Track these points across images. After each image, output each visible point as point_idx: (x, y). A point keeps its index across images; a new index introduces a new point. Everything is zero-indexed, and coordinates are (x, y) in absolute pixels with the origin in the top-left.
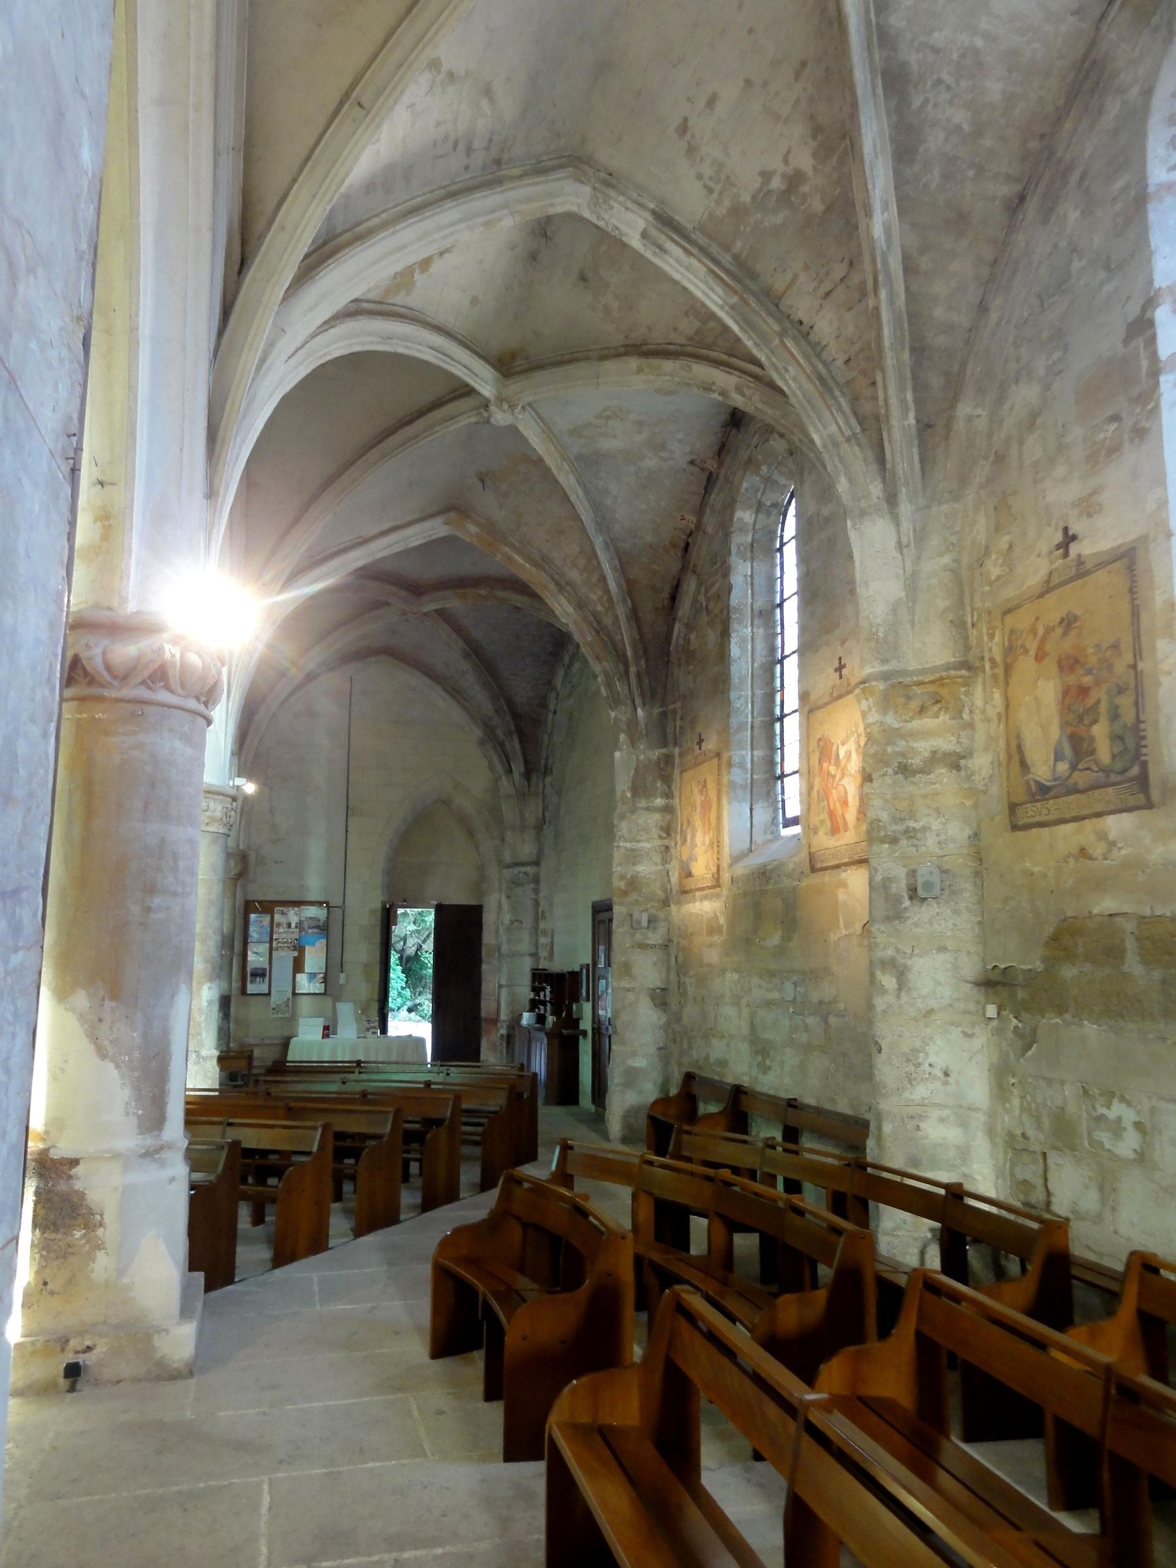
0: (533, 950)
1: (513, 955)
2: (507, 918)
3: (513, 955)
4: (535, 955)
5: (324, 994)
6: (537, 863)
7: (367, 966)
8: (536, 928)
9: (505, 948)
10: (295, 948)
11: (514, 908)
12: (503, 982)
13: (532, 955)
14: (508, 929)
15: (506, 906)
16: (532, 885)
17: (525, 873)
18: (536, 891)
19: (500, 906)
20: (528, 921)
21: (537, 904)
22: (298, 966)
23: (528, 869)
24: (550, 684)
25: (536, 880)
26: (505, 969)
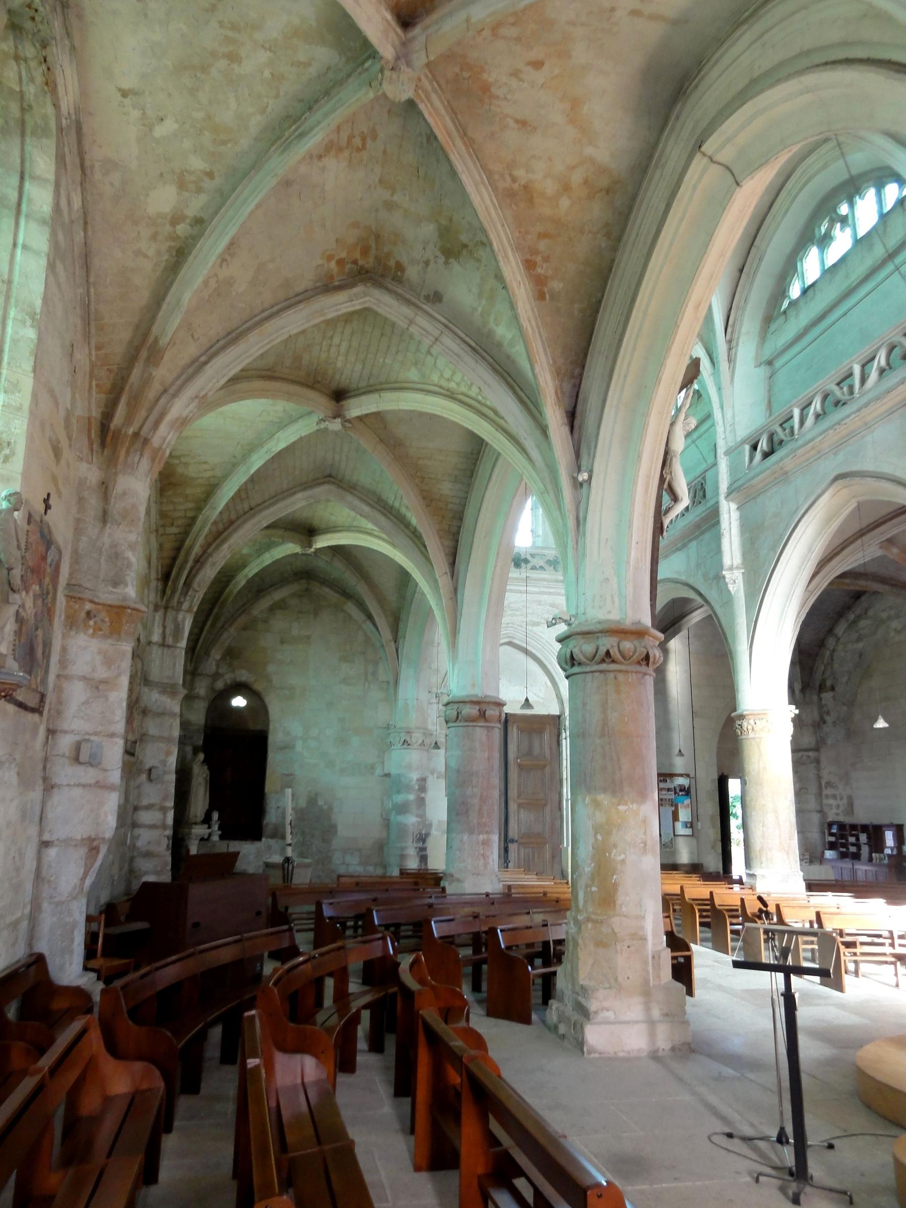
0: (818, 808)
4: (821, 811)
5: (692, 835)
6: (817, 749)
7: (712, 817)
8: (820, 794)
10: (672, 805)
16: (814, 764)
17: (809, 757)
20: (813, 789)
21: (819, 778)
22: (675, 817)
23: (812, 754)
24: (830, 631)
25: (818, 761)
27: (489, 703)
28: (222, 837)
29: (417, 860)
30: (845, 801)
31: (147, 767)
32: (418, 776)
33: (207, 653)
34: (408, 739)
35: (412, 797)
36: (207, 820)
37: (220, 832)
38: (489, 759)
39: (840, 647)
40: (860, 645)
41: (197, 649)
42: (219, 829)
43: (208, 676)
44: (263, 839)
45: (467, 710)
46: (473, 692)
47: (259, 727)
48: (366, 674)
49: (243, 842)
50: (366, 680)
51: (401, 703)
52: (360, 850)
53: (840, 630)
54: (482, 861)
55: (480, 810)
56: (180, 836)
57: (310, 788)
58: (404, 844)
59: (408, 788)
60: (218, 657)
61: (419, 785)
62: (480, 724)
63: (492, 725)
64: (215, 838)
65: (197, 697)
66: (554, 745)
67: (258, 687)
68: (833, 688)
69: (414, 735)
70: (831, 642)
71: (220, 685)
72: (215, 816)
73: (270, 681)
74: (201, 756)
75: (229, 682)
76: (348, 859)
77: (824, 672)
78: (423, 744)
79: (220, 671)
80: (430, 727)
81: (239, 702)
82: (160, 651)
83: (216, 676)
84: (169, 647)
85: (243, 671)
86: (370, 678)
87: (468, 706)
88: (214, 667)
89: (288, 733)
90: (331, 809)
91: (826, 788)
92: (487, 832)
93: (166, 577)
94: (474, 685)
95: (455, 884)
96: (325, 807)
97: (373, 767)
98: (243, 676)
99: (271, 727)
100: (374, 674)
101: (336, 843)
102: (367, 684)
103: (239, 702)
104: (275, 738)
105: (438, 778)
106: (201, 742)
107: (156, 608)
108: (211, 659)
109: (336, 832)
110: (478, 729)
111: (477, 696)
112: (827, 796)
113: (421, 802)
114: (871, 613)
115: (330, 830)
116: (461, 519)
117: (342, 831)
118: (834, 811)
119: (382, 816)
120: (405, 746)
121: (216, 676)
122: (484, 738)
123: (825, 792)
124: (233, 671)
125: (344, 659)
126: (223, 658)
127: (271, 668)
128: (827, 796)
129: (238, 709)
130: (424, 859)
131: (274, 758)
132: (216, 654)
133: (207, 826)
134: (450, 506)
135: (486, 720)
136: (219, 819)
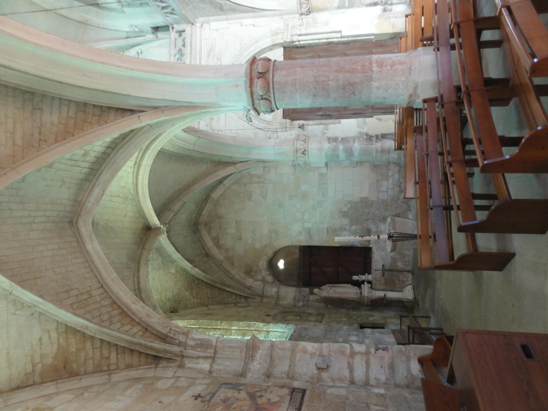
27: (251, 70)
28: (369, 273)
29: (385, 140)
31: (316, 372)
32: (327, 143)
33: (249, 288)
34: (301, 151)
35: (341, 147)
36: (358, 284)
37: (366, 274)
38: (302, 67)
41: (246, 295)
42: (364, 275)
43: (264, 286)
44: (371, 246)
45: (259, 90)
46: (243, 86)
47: (297, 251)
48: (259, 182)
49: (373, 260)
50: (263, 182)
51: (277, 158)
52: (378, 181)
54: (397, 66)
55: (350, 72)
56: (369, 303)
57: (337, 217)
58: (374, 151)
59: (335, 150)
60: (252, 280)
61: (333, 142)
62: (271, 77)
63: (272, 66)
64: (370, 277)
65: (278, 293)
66: (303, 50)
67: (270, 254)
69: (298, 147)
71: (270, 278)
72: (355, 278)
73: (266, 246)
74: (316, 290)
75: (268, 273)
76: (384, 188)
78: (304, 141)
79: (260, 278)
80: (294, 137)
81: (281, 264)
82: (219, 361)
83: (264, 281)
84: (215, 353)
85: (260, 264)
86: (262, 180)
87: (255, 89)
88: (258, 283)
89: (300, 233)
90: (350, 202)
92: (371, 64)
93: (156, 359)
94: (237, 86)
95: (419, 92)
96: (349, 206)
97: (321, 175)
98: (263, 263)
99: (296, 244)
100: (259, 177)
101: (373, 198)
102: (267, 182)
103: (281, 264)
104: (304, 241)
105: (328, 130)
106: (307, 289)
107: (181, 366)
108: (253, 285)
109: (366, 198)
110: (276, 79)
111: (245, 82)
113: (344, 140)
115: (365, 202)
116: (85, 104)
117: (364, 195)
119: (354, 167)
120: (306, 153)
121: (264, 281)
122: (284, 72)
124: (260, 271)
125: (250, 198)
126: (252, 277)
127: (258, 246)
129: (285, 264)
130: (384, 136)
131: (316, 242)
132: (250, 282)
133: (362, 286)
134: (71, 114)
135: (267, 71)
136: (358, 275)
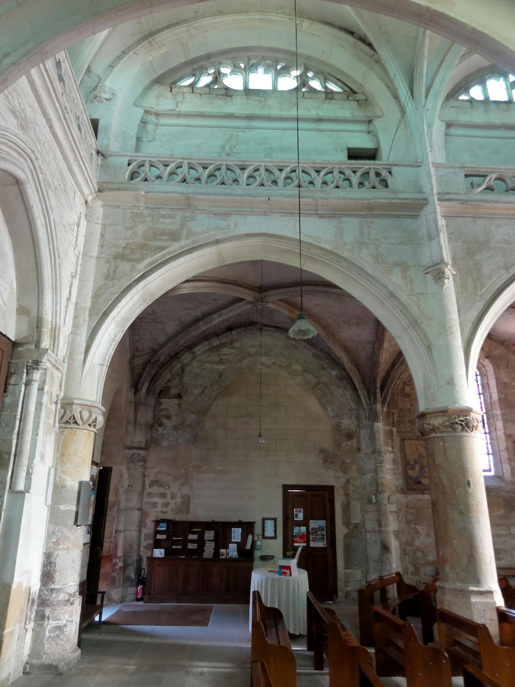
0: (139, 506)
1: (127, 509)
2: (126, 483)
3: (127, 509)
9: (123, 504)
11: (130, 477)
12: (121, 527)
13: (140, 509)
14: (127, 492)
15: (126, 476)
17: (139, 455)
18: (144, 467)
19: (121, 476)
20: (138, 487)
25: (144, 460)
26: (122, 519)
30: (179, 500)
39: (195, 364)
40: (221, 367)
53: (199, 350)
68: (179, 396)
70: (186, 357)
77: (169, 381)
91: (150, 486)
112: (150, 495)
114: (237, 344)
118: (160, 508)
123: (148, 490)
128: (150, 495)
